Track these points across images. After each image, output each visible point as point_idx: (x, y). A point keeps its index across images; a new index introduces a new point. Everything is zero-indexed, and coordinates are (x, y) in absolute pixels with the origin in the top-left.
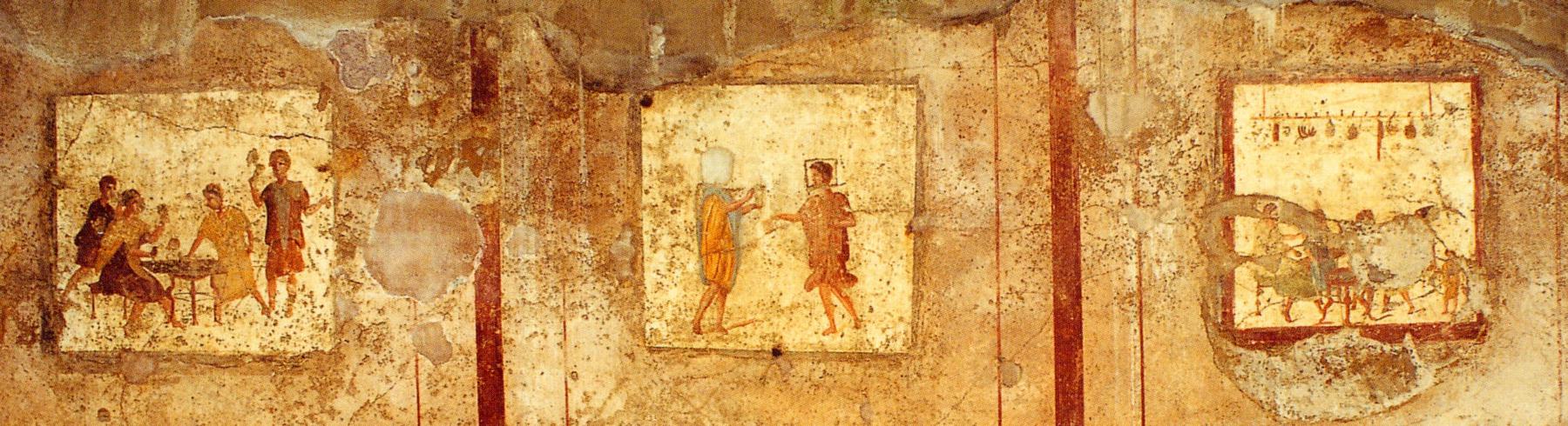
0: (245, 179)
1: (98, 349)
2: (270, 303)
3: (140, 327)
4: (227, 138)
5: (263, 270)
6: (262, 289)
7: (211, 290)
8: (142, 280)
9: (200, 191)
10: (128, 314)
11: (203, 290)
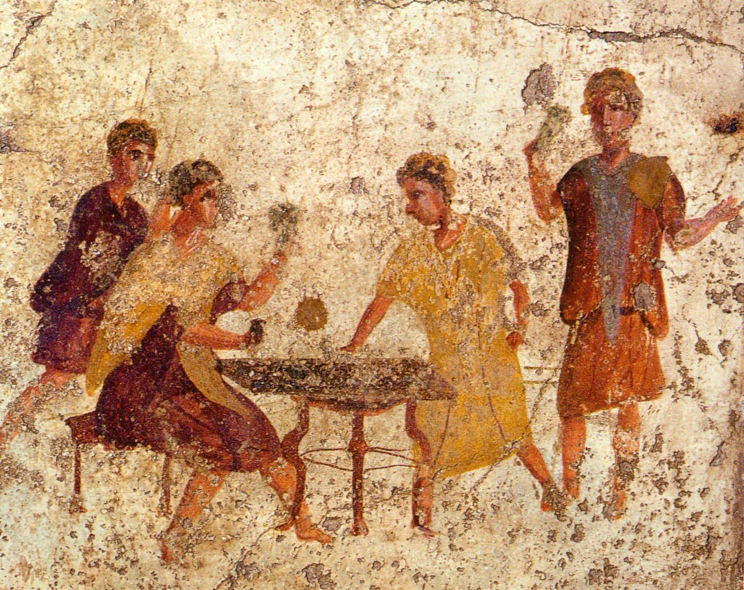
5: (552, 393)
7: (406, 442)
8: (215, 410)
9: (390, 173)
10: (174, 503)
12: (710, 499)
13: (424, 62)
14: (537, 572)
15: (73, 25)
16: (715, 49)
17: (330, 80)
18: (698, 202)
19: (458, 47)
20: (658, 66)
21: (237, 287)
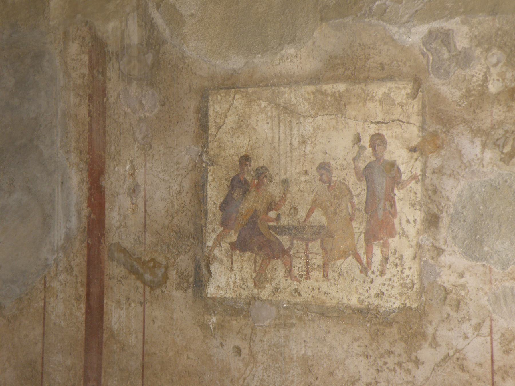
0: (350, 158)
1: (234, 297)
3: (266, 280)
4: (337, 123)
5: (363, 236)
7: (321, 251)
8: (268, 241)
9: (314, 168)
10: (257, 269)
11: (314, 250)
12: (412, 270)
13: (323, 134)
14: (360, 293)
15: (229, 127)
16: (409, 125)
17: (297, 141)
18: (406, 175)
19: (332, 129)
20: (391, 131)
21: (273, 203)
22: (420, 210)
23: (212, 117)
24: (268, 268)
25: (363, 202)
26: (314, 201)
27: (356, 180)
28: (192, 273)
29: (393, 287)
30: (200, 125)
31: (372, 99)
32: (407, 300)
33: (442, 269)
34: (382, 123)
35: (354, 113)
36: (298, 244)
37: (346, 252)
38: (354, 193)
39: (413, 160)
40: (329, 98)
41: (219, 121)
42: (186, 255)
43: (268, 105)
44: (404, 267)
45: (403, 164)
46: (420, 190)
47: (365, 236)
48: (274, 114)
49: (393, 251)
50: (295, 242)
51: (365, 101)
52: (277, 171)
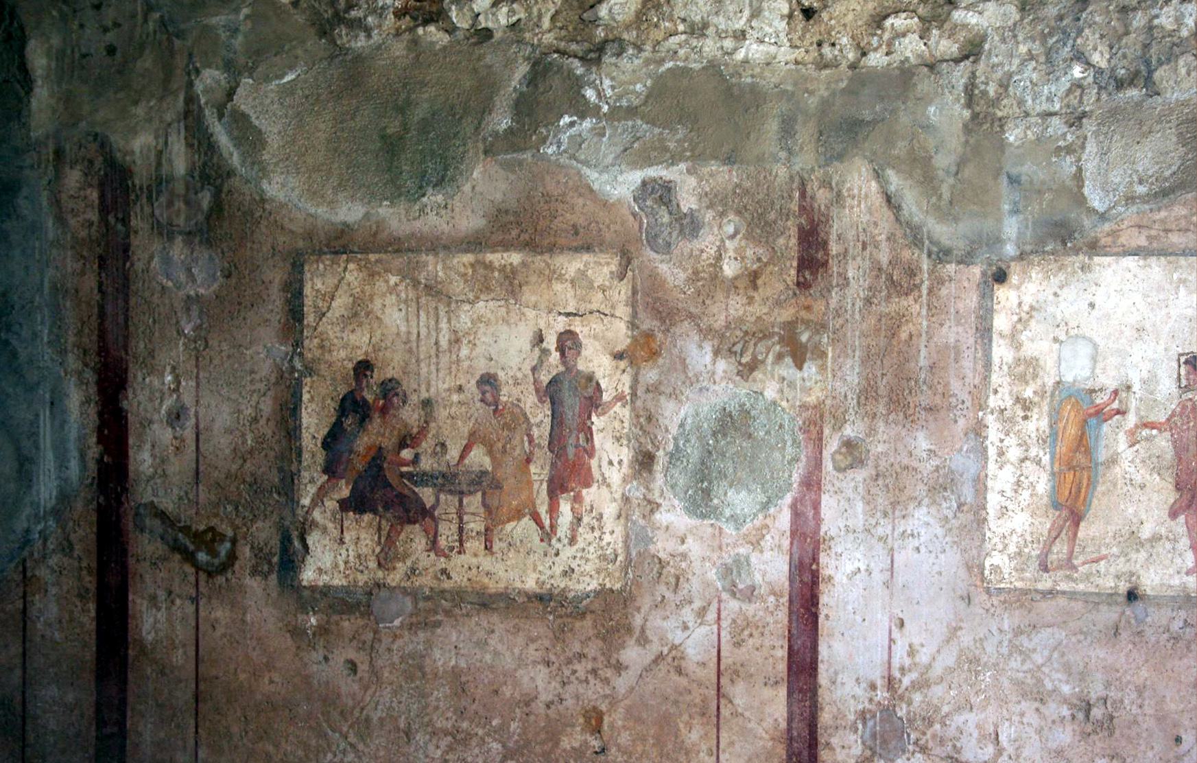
1: (345, 584)
2: (552, 526)
5: (545, 486)
6: (543, 510)
7: (482, 510)
8: (401, 496)
9: (473, 382)
10: (383, 540)
11: (472, 509)
12: (614, 536)
22: (628, 447)
23: (310, 298)
24: (401, 538)
25: (547, 434)
26: (472, 434)
27: (536, 400)
28: (277, 550)
29: (587, 560)
30: (290, 310)
31: (560, 278)
32: (607, 579)
33: (656, 532)
34: (575, 315)
35: (533, 299)
36: (446, 499)
37: (520, 511)
38: (532, 421)
39: (619, 372)
40: (496, 274)
41: (320, 305)
42: (267, 521)
43: (401, 281)
44: (604, 530)
45: (604, 377)
46: (628, 416)
47: (548, 486)
48: (410, 296)
49: (589, 508)
50: (442, 497)
51: (550, 281)
52: (416, 387)
